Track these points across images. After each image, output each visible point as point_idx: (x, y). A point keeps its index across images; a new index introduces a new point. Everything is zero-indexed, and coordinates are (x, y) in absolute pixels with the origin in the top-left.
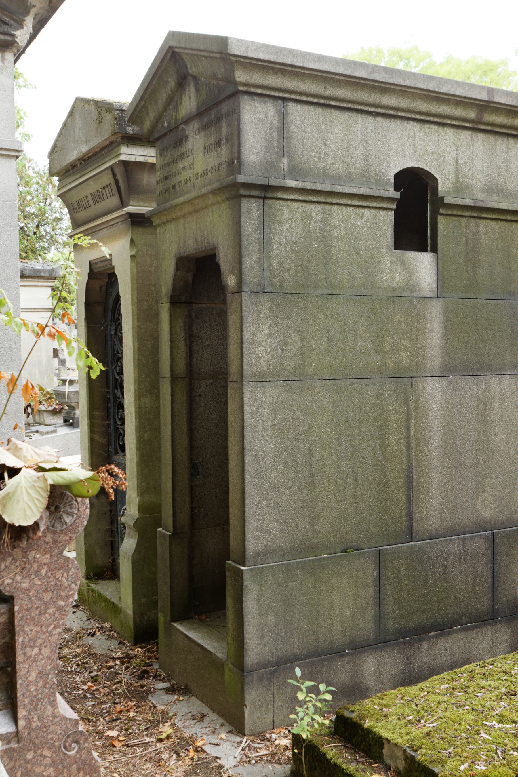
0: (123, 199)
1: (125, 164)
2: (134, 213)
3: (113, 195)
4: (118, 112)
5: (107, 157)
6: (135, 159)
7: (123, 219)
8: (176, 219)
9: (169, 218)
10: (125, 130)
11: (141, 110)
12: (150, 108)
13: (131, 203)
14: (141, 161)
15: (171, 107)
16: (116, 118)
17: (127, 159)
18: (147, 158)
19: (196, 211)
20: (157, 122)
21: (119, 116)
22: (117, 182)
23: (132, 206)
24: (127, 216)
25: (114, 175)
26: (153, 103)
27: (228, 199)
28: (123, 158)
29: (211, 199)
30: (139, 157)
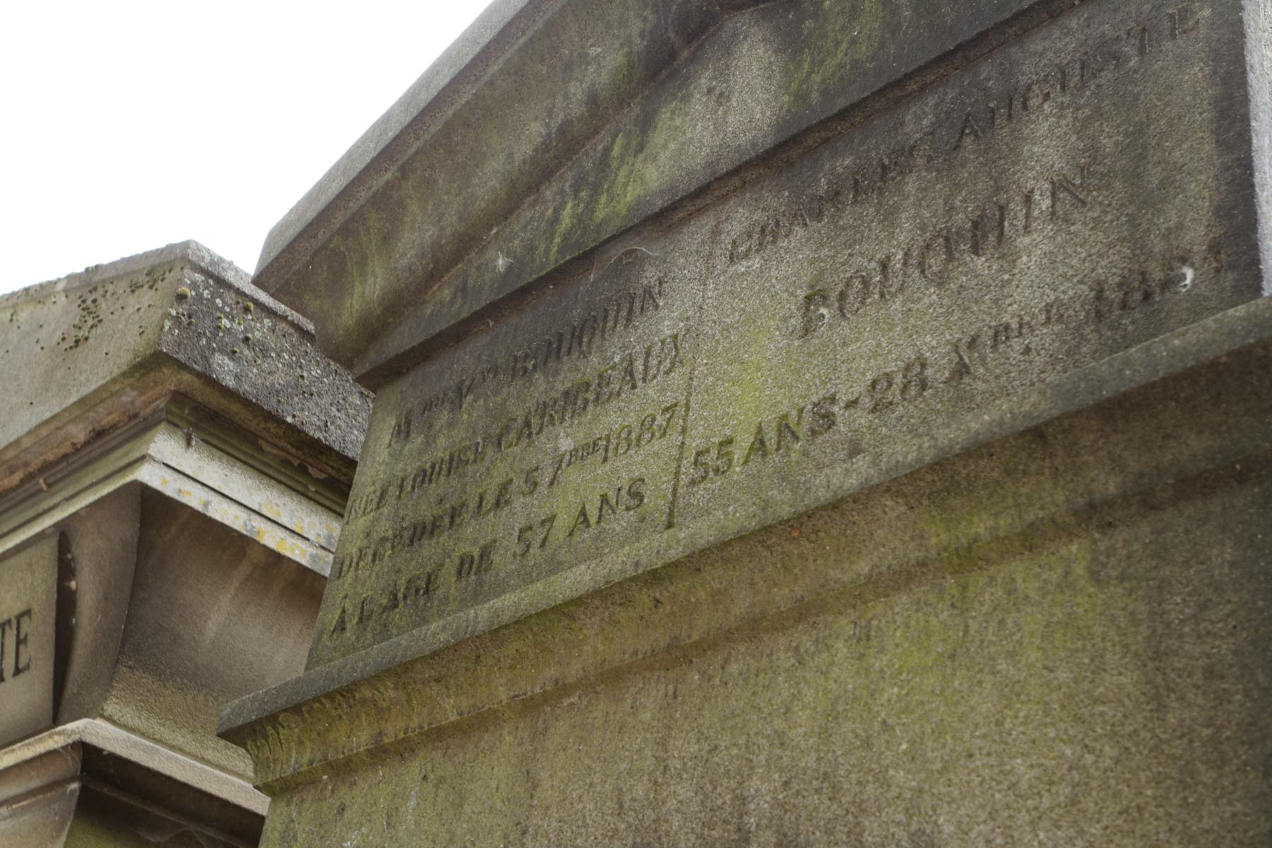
0: (71, 688)
1: (152, 509)
2: (113, 757)
3: (18, 671)
4: (199, 277)
5: (53, 495)
6: (206, 504)
7: (35, 783)
8: (477, 723)
9: (393, 730)
10: (206, 359)
11: (359, 216)
12: (414, 207)
13: (111, 708)
14: (228, 522)
15: (567, 177)
16: (181, 298)
17: (169, 491)
18: (257, 522)
19: (678, 656)
20: (433, 277)
21: (199, 295)
22: (65, 603)
23: (110, 719)
24: (71, 764)
25: (65, 569)
26: (441, 180)
27: (1094, 515)
28: (149, 475)
29: (890, 539)
30: (225, 504)
